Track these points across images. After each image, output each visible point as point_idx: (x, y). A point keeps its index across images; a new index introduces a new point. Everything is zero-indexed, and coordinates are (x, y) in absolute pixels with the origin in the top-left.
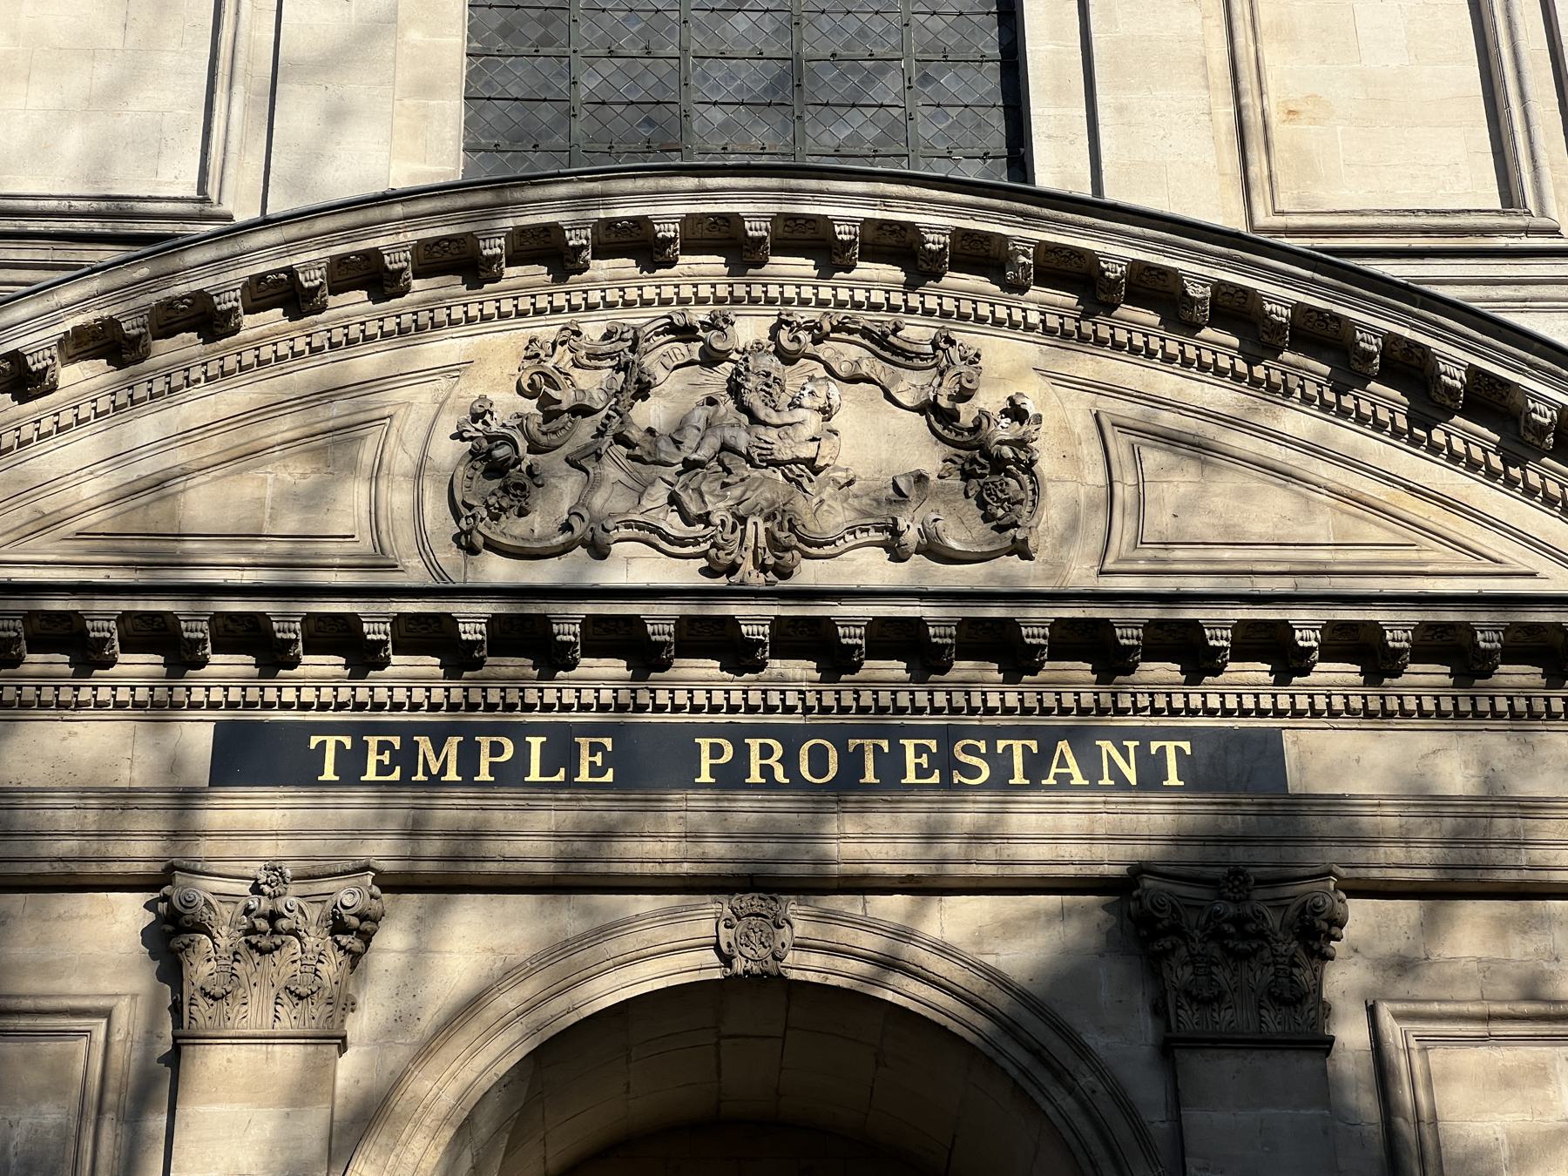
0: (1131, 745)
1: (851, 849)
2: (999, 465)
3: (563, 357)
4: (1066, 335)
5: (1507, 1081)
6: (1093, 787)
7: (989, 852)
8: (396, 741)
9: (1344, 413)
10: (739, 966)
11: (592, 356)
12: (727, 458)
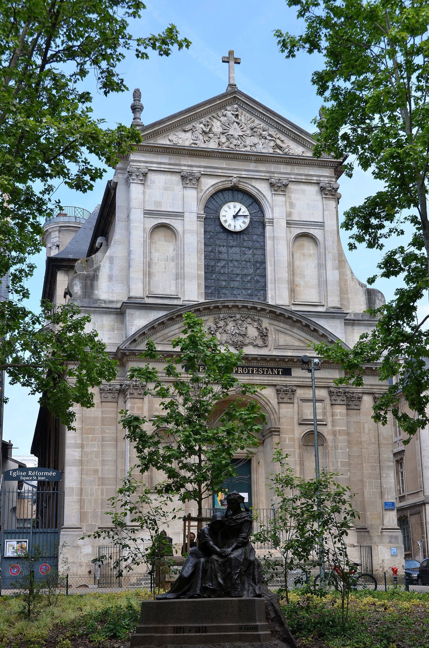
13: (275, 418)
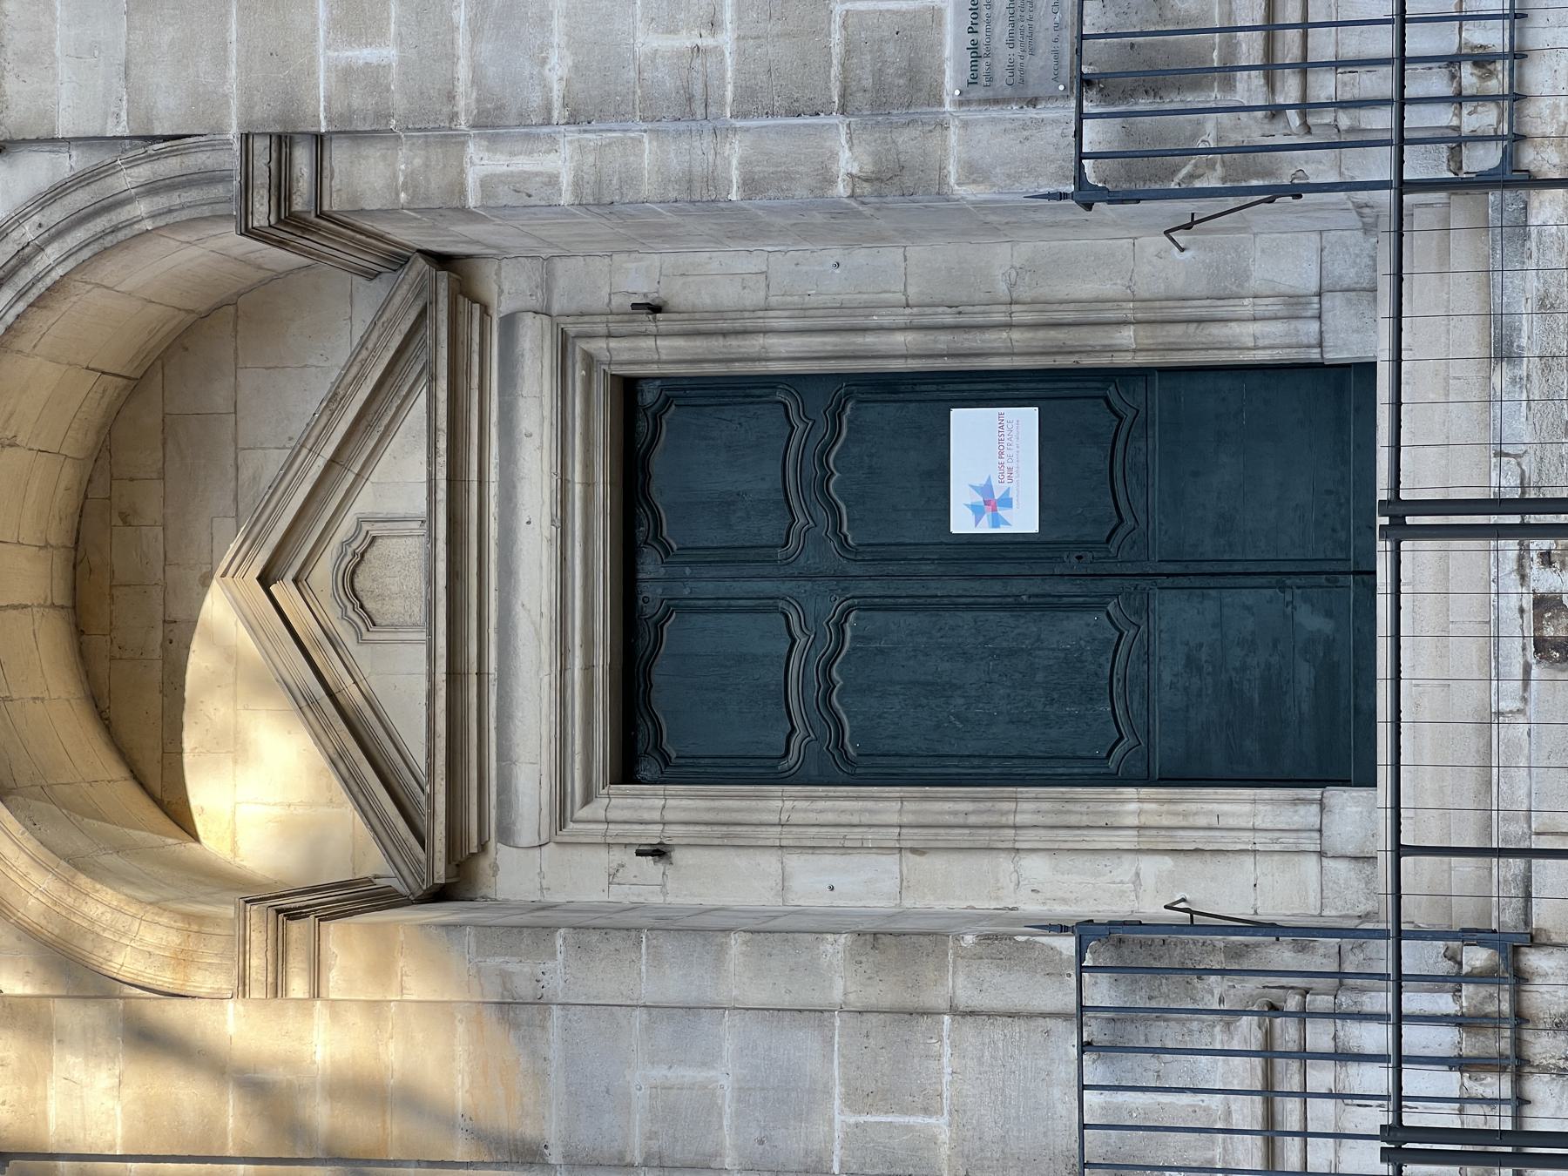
13: (151, 189)
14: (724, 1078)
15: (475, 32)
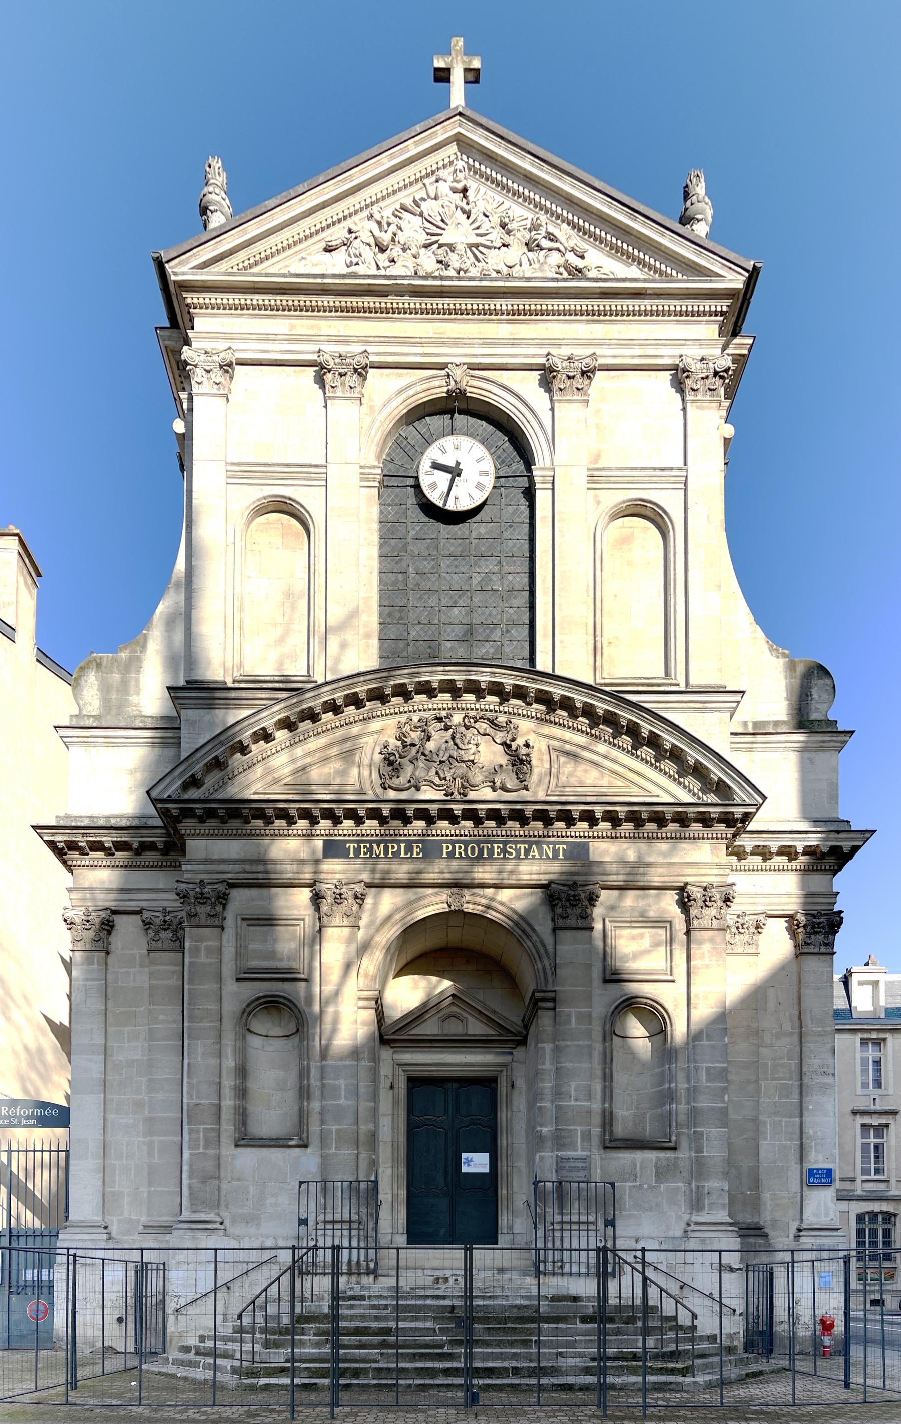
0: (551, 846)
1: (480, 875)
2: (522, 762)
3: (407, 727)
4: (542, 720)
5: (633, 938)
6: (541, 859)
7: (514, 876)
8: (368, 845)
9: (614, 745)
10: (453, 908)
11: (415, 727)
12: (451, 760)
13: (544, 968)
14: (342, 1102)
15: (577, 1046)
